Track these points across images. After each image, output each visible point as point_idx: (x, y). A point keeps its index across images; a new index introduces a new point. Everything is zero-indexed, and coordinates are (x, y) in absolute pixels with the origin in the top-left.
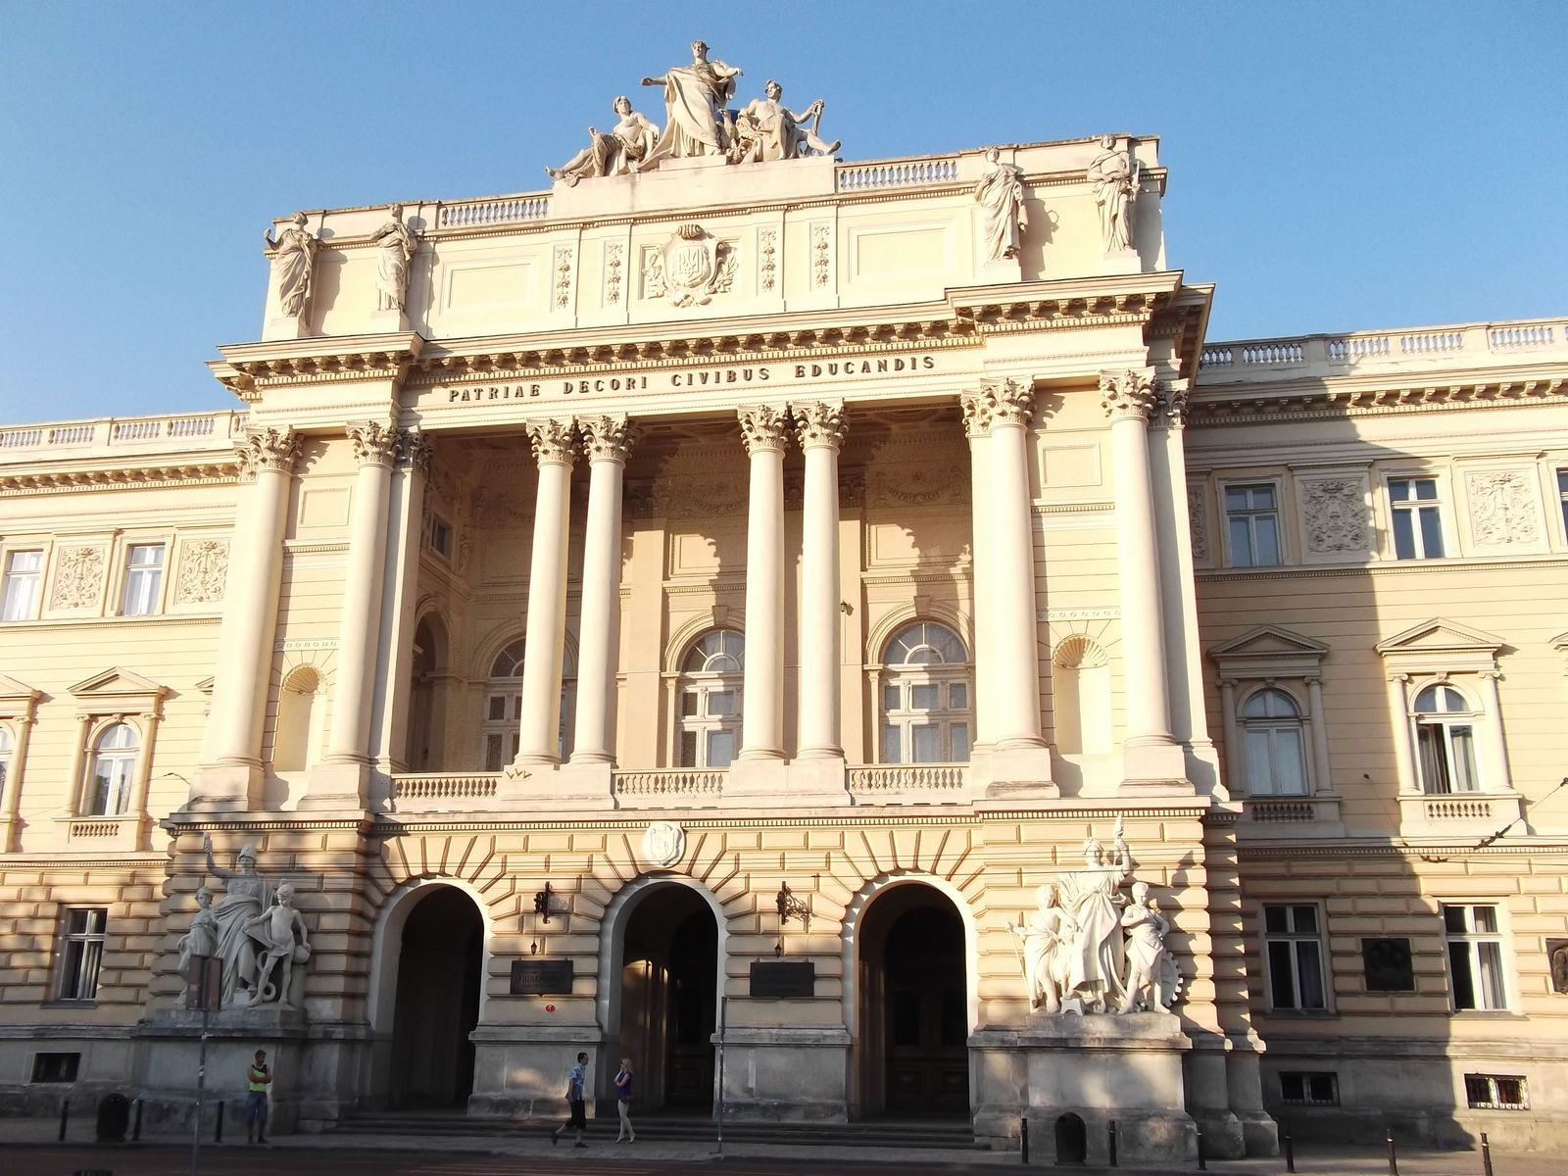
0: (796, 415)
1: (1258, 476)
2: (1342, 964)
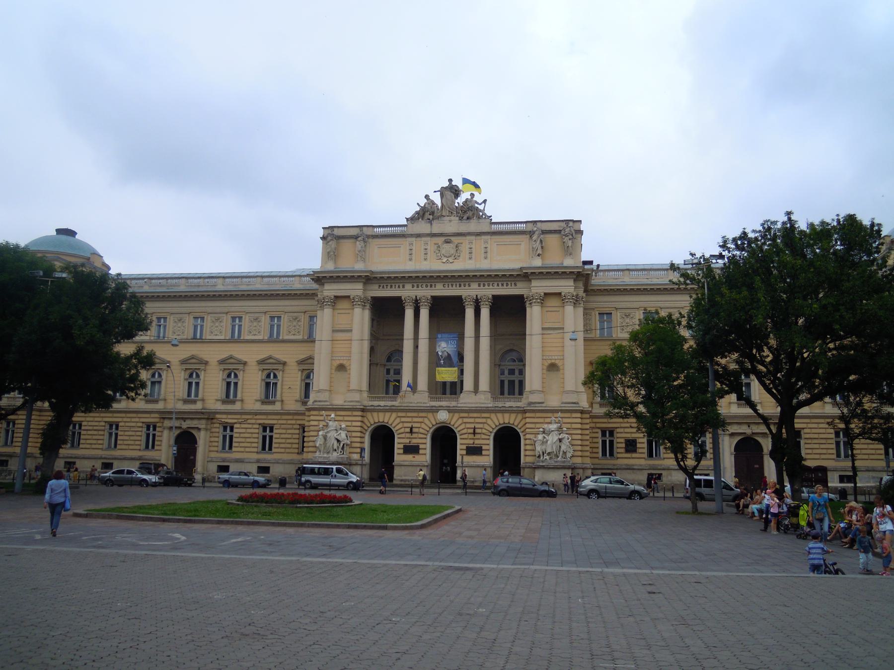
1: (607, 310)
2: (619, 445)
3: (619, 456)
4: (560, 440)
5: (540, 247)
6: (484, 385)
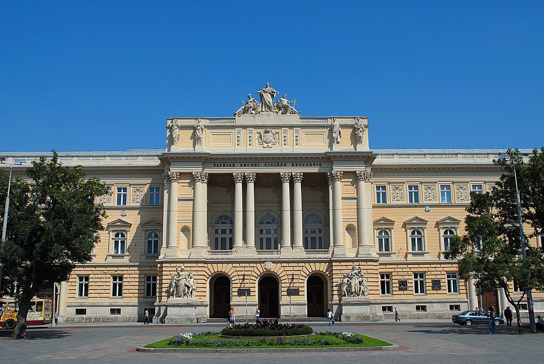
0: (293, 174)
3: (394, 293)
4: (360, 283)
5: (339, 137)
6: (300, 241)
